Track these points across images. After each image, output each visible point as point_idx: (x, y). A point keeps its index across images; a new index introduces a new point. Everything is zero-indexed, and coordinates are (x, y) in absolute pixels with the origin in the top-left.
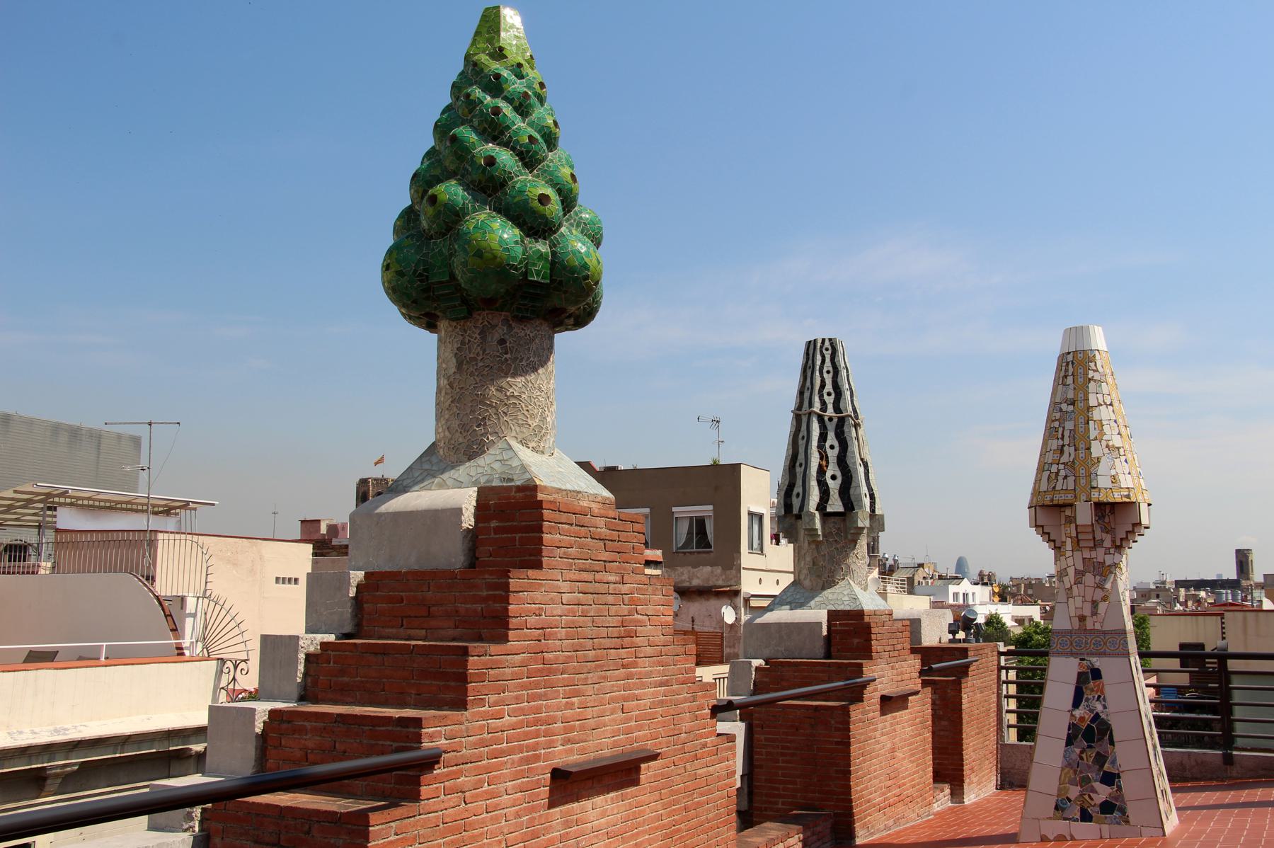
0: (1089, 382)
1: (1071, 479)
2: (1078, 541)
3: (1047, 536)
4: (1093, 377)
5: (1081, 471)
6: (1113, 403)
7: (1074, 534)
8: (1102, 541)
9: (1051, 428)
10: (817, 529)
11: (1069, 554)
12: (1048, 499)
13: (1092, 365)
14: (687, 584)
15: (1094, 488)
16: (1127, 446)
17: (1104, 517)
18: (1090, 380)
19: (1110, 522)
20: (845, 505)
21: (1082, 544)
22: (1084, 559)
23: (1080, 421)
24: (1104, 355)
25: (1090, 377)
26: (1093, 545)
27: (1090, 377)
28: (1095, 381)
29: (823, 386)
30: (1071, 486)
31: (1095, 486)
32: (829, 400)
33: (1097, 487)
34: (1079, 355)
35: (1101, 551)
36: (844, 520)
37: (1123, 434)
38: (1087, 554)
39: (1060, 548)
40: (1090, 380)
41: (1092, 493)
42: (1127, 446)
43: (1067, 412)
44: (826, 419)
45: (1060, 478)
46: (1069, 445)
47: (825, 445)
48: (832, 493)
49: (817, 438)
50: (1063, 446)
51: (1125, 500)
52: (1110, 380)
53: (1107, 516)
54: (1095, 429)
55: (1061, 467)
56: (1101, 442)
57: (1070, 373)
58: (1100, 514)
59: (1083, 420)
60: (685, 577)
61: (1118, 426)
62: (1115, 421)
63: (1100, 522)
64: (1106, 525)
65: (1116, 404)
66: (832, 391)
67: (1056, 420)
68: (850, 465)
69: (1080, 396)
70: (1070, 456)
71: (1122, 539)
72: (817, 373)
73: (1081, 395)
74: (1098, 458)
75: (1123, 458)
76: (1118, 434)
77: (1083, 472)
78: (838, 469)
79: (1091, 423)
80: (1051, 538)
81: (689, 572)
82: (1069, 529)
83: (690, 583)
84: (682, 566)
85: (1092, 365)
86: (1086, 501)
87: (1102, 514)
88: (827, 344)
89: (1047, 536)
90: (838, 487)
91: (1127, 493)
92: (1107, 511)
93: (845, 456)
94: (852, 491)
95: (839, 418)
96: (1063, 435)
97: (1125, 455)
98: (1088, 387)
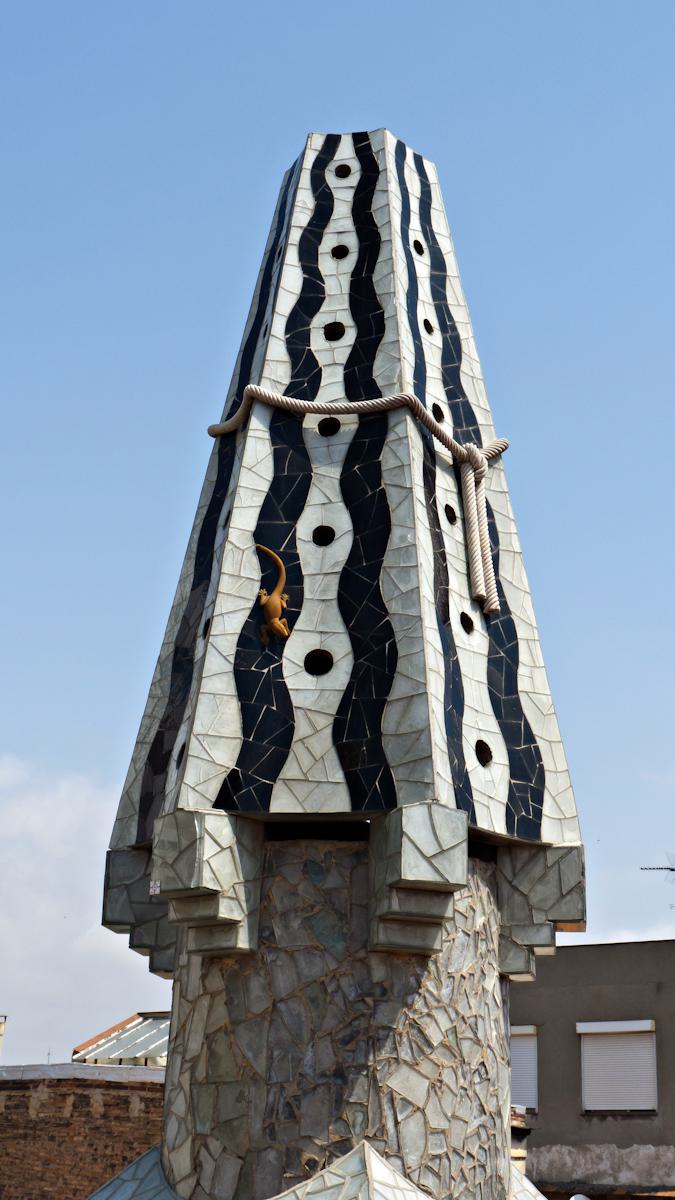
10: (212, 896)
14: (608, 1181)
20: (356, 787)
29: (312, 296)
32: (331, 357)
36: (360, 857)
44: (311, 423)
47: (292, 528)
48: (301, 728)
49: (259, 501)
60: (605, 1166)
66: (346, 319)
68: (393, 607)
72: (292, 256)
78: (340, 627)
81: (612, 1155)
83: (616, 1179)
84: (600, 1142)
88: (346, 153)
90: (333, 703)
93: (375, 570)
94: (390, 721)
95: (363, 415)
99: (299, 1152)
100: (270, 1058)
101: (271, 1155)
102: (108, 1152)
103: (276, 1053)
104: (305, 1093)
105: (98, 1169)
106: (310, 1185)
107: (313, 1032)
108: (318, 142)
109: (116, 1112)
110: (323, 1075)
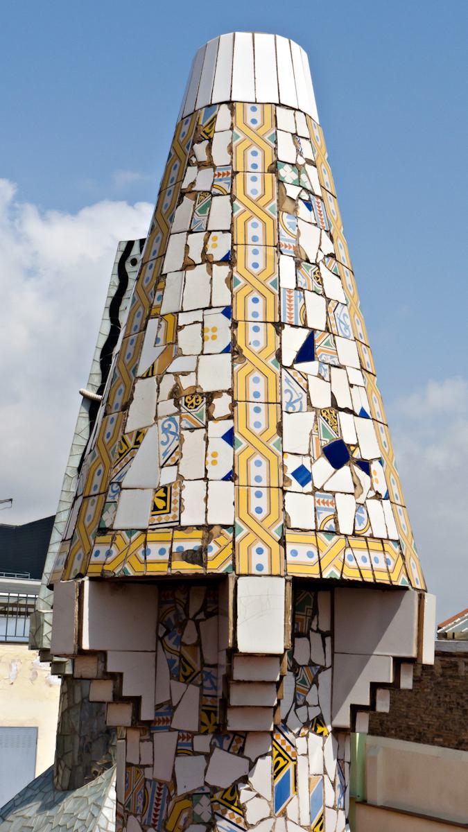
0: (180, 201)
4: (193, 184)
6: (240, 256)
13: (200, 149)
15: (103, 531)
17: (182, 626)
18: (183, 194)
19: (199, 644)
27: (185, 185)
31: (108, 525)
33: (111, 529)
35: (165, 741)
41: (95, 549)
52: (254, 187)
54: (157, 340)
56: (159, 381)
58: (171, 616)
61: (235, 325)
62: (228, 312)
63: (170, 642)
65: (249, 258)
75: (218, 429)
76: (226, 350)
79: (153, 323)
85: (200, 149)
87: (176, 616)
92: (195, 606)
97: (230, 417)
98: (172, 219)
99: (91, 768)
100: (81, 725)
101: (80, 769)
102: (447, 699)
103: (83, 722)
104: (94, 741)
105: (442, 710)
106: (93, 783)
107: (97, 713)
108: (123, 247)
109: (449, 672)
110: (101, 732)
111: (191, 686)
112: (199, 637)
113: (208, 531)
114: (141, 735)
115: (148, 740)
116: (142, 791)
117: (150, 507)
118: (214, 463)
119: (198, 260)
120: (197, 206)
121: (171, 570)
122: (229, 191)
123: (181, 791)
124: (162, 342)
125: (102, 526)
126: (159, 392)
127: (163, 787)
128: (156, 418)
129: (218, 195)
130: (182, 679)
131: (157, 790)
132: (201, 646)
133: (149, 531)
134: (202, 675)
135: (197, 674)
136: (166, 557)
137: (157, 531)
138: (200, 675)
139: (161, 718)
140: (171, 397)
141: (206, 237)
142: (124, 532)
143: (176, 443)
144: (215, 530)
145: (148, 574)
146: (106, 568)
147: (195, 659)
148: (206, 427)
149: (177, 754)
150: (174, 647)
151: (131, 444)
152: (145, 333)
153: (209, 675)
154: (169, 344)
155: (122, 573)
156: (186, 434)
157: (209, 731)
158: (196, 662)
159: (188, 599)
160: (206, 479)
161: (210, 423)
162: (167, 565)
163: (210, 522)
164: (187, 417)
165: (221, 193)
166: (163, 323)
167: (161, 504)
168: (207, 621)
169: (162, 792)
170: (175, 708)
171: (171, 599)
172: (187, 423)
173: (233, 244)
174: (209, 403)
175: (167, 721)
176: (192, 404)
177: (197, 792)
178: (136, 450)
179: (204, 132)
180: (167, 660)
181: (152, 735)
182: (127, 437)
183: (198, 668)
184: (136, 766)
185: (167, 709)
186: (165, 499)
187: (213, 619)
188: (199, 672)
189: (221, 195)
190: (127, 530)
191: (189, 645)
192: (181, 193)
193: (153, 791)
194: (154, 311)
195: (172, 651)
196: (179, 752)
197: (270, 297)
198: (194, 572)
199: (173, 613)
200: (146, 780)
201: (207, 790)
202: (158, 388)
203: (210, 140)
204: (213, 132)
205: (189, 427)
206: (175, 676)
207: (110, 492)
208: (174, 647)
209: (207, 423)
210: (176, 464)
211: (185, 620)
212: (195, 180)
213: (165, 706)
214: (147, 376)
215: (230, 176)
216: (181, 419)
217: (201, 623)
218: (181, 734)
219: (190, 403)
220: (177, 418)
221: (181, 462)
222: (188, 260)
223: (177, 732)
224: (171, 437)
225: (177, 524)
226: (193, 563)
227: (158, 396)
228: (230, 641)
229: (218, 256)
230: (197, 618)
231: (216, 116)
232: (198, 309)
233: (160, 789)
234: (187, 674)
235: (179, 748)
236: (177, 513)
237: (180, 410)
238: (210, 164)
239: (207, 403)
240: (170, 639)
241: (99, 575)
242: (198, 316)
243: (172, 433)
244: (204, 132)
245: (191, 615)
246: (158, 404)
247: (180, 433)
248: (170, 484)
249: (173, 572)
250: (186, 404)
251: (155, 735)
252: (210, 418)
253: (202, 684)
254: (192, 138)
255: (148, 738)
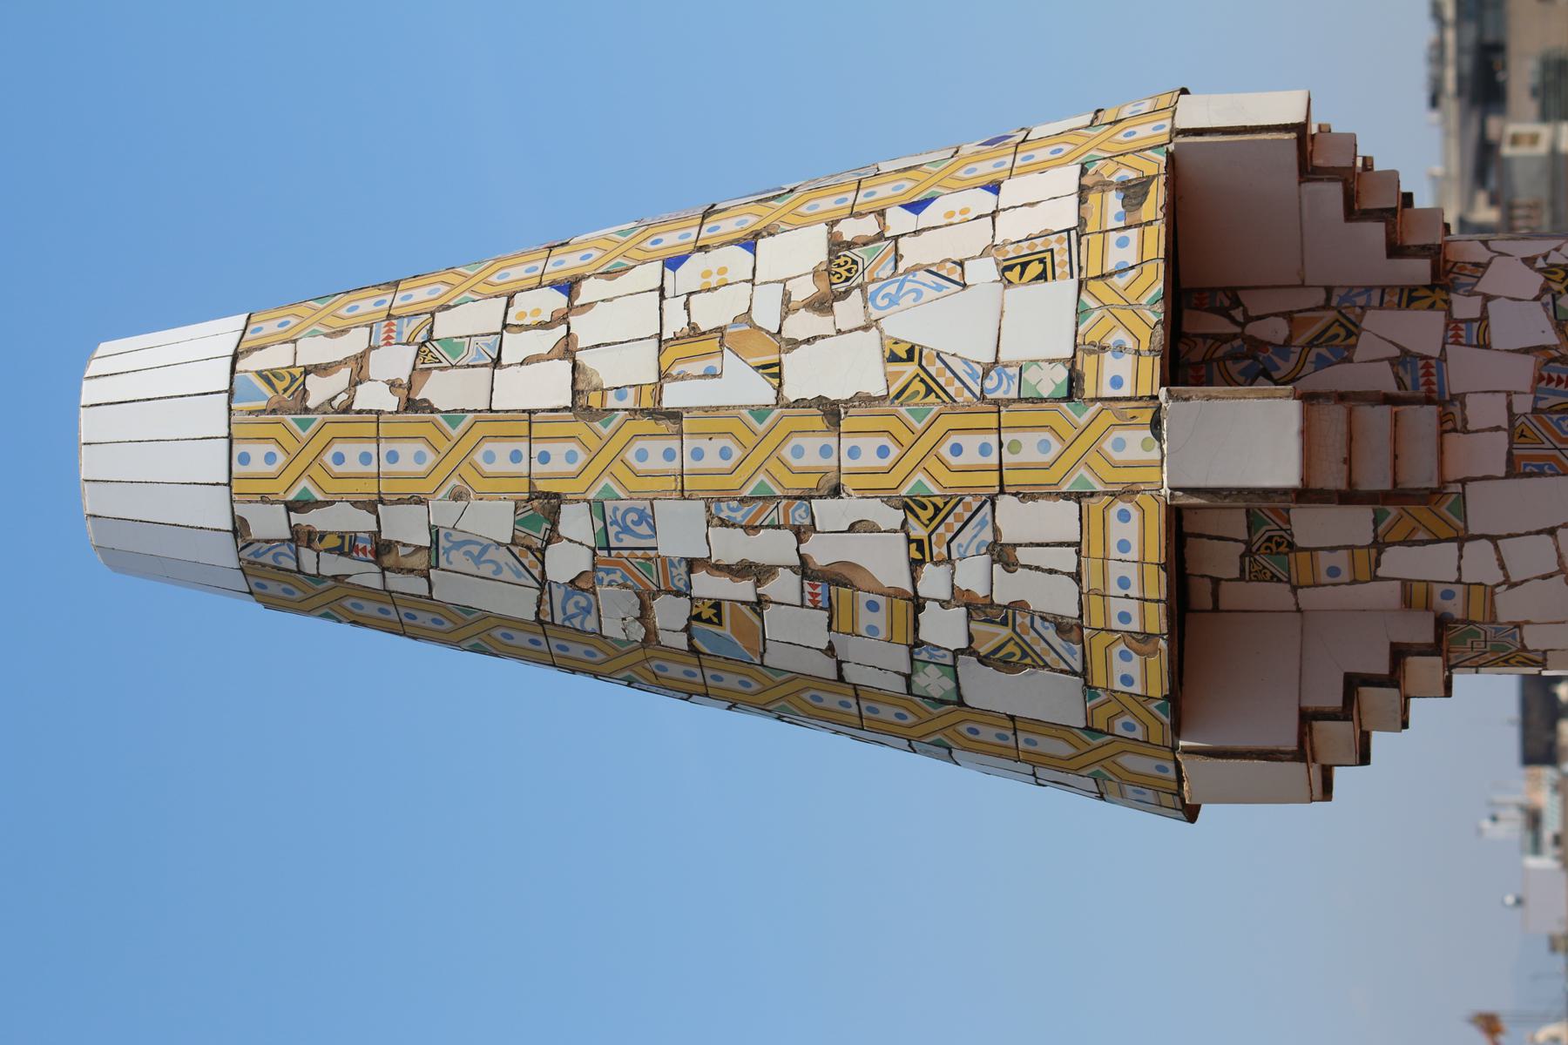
0: (427, 407)
1: (1015, 520)
2: (1398, 495)
3: (1368, 694)
4: (393, 385)
5: (970, 457)
7: (1355, 524)
8: (1403, 359)
9: (693, 650)
11: (1479, 563)
12: (1134, 667)
13: (319, 390)
15: (1074, 381)
16: (827, 204)
17: (1257, 345)
18: (411, 405)
19: (1288, 316)
21: (1421, 475)
22: (1513, 470)
23: (656, 462)
24: (270, 327)
25: (390, 402)
26: (1432, 410)
28: (419, 372)
30: (1060, 519)
31: (1062, 374)
34: (258, 466)
37: (751, 222)
38: (1490, 452)
39: (1442, 623)
40: (411, 405)
42: (827, 204)
43: (604, 544)
45: (1007, 588)
46: (800, 533)
50: (804, 569)
51: (1154, 204)
53: (1252, 329)
54: (710, 374)
55: (933, 582)
56: (794, 344)
57: (362, 522)
59: (656, 447)
61: (703, 249)
64: (1302, 340)
67: (644, 615)
69: (503, 465)
70: (873, 528)
71: (1396, 250)
73: (500, 458)
74: (894, 358)
77: (971, 443)
79: (674, 396)
80: (1382, 667)
82: (1325, 560)
85: (319, 390)
86: (1156, 425)
89: (1368, 694)
91: (1114, 201)
92: (1222, 326)
96: (741, 570)
97: (881, 214)
98: (455, 415)
111: (1364, 325)
112: (1276, 315)
113: (1090, 188)
114: (1455, 430)
115: (1463, 405)
116: (1555, 417)
117: (1041, 285)
118: (963, 212)
119: (561, 330)
120: (445, 363)
121: (1156, 220)
122: (429, 315)
123: (1551, 338)
124: (714, 362)
125: (1065, 394)
126: (815, 338)
127: (1545, 374)
128: (866, 328)
129: (431, 331)
130: (1352, 340)
131: (1552, 385)
132: (1292, 312)
133: (1083, 275)
134: (1346, 308)
135: (1348, 319)
136: (1133, 234)
137: (1083, 264)
138: (1343, 311)
139: (1422, 381)
140: (829, 310)
141: (515, 329)
142: (1081, 329)
143: (922, 276)
144: (1087, 181)
145: (1162, 255)
146: (1144, 346)
147: (1315, 321)
148: (896, 238)
149: (1487, 346)
150: (1294, 358)
151: (911, 369)
152: (688, 410)
153: (1342, 299)
154: (721, 345)
155: (1159, 308)
156: (902, 266)
157: (1445, 297)
158: (1321, 318)
159: (1205, 336)
160: (994, 215)
161: (887, 235)
162: (1147, 228)
163: (1075, 188)
164: (871, 272)
165: (428, 327)
166: (674, 372)
167: (1034, 269)
168: (1245, 303)
169: (1555, 376)
170: (1405, 352)
171: (1203, 372)
172: (883, 269)
173: (540, 285)
174: (850, 245)
175: (1427, 366)
176: (849, 271)
177: (1551, 313)
178: (925, 352)
179: (285, 390)
180: (1316, 371)
181: (1454, 397)
182: (894, 390)
183: (1330, 316)
184: (1511, 443)
185: (1405, 369)
186: (1024, 265)
187: (1242, 295)
188: (1340, 312)
189: (432, 328)
190: (1077, 325)
191: (1290, 331)
192: (406, 410)
193: (1555, 393)
194: (648, 403)
195: (1301, 363)
196: (1482, 343)
197: (651, 231)
198: (1162, 189)
199: (1229, 364)
200: (1535, 410)
201: (1547, 298)
202: (808, 341)
203: (307, 371)
204: (292, 370)
205: (892, 263)
206: (1346, 354)
207: (999, 395)
208: (1294, 358)
209: (888, 238)
210: (961, 264)
211: (1243, 340)
212: (387, 382)
213: (1401, 373)
214: (779, 375)
215: (395, 321)
216: (873, 281)
217: (1252, 313)
218: (1450, 340)
219: (845, 274)
220: (871, 288)
221: (957, 259)
222: (556, 351)
223: (1448, 347)
224: (908, 286)
225: (1073, 233)
226: (1146, 194)
227: (823, 337)
228: (1286, 136)
229: (561, 300)
230: (1240, 318)
231: (259, 373)
232: (660, 308)
233: (1550, 380)
234: (1343, 333)
235: (1475, 342)
236: (1053, 238)
237: (859, 286)
238: (360, 361)
239: (849, 249)
240: (1278, 368)
241: (1158, 359)
242: (674, 307)
243: (900, 288)
244: (285, 390)
245: (1238, 330)
246: (839, 332)
247: (901, 275)
248: (997, 264)
249: (1160, 215)
250: (847, 279)
251: (1454, 391)
252: (880, 237)
253: (1362, 307)
254: (288, 418)
255: (1457, 403)
